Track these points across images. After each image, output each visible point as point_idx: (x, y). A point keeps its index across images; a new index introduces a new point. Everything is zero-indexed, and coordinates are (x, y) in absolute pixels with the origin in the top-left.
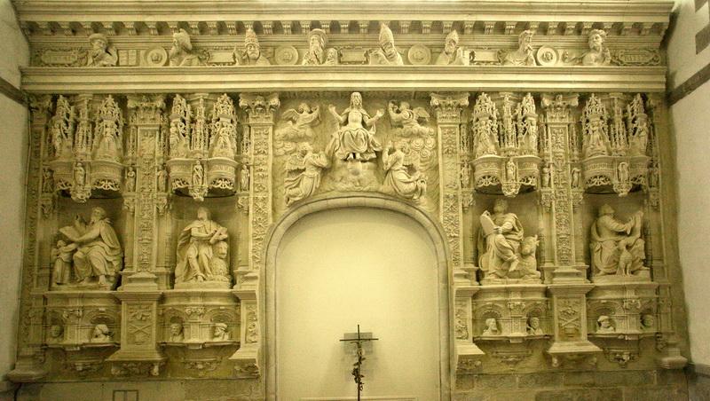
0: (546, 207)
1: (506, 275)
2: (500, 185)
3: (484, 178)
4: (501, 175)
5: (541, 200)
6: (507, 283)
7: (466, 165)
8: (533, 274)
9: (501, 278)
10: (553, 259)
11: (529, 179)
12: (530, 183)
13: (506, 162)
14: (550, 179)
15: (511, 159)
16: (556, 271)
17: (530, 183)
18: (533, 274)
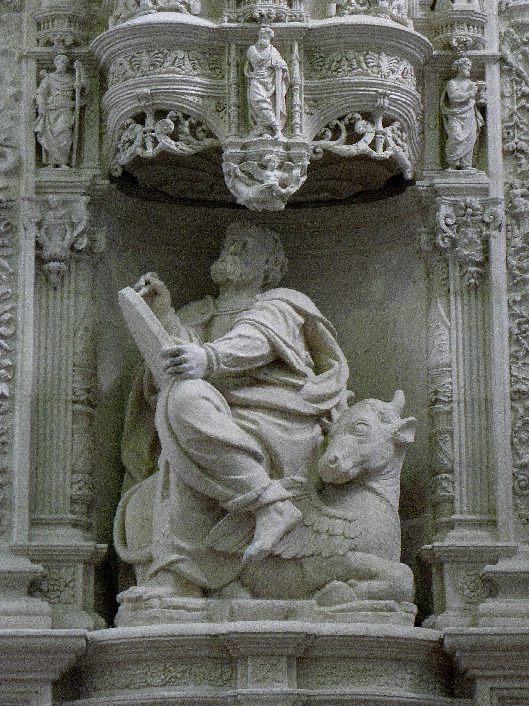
0: (463, 263)
1: (239, 579)
2: (218, 150)
3: (140, 119)
4: (220, 109)
5: (435, 232)
6: (232, 617)
7: (60, 61)
8: (371, 576)
9: (206, 593)
10: (493, 511)
11: (361, 125)
12: (363, 146)
13: (243, 50)
14: (483, 133)
15: (267, 28)
16: (503, 565)
17: (363, 146)
18: (371, 576)
